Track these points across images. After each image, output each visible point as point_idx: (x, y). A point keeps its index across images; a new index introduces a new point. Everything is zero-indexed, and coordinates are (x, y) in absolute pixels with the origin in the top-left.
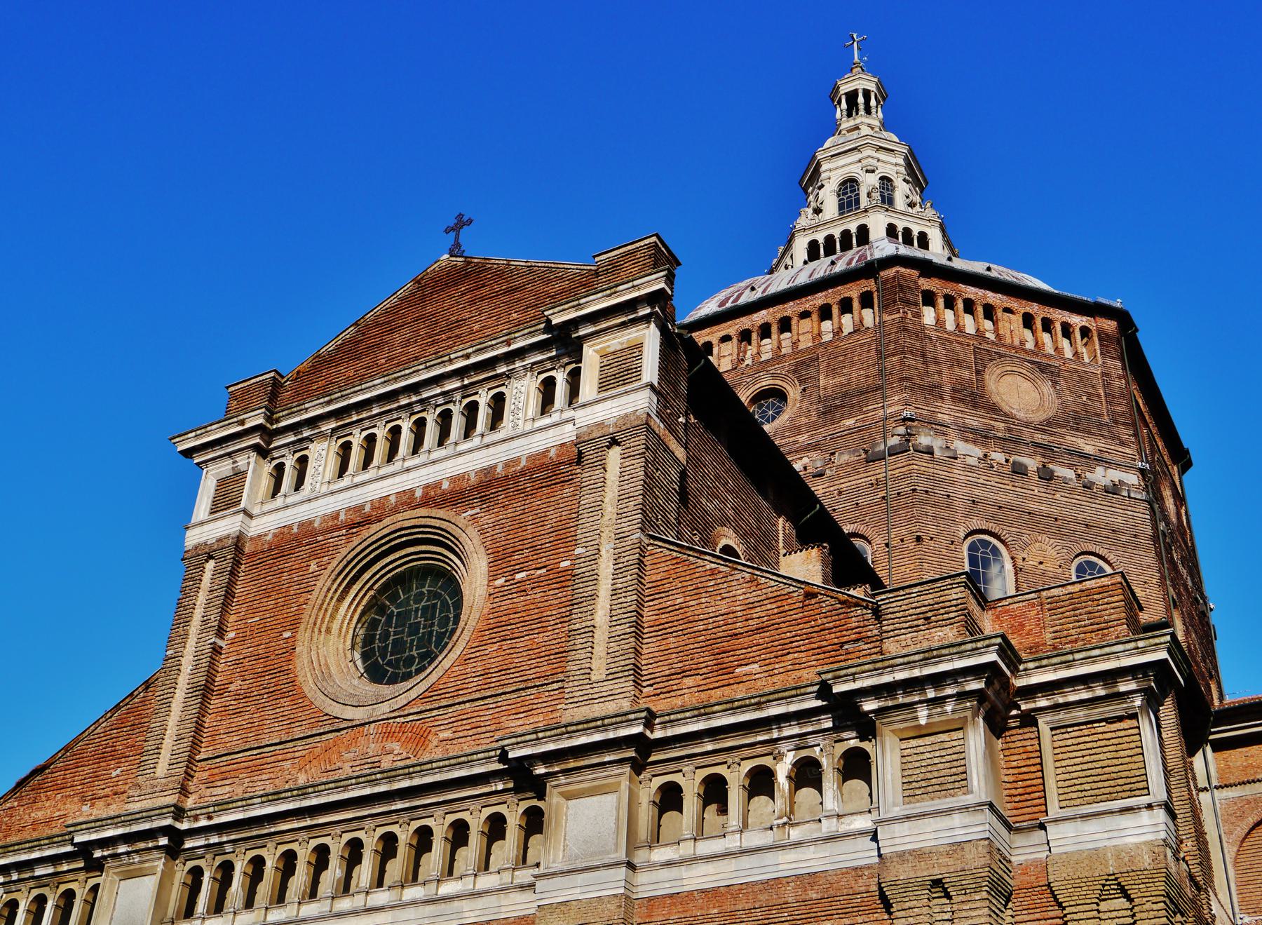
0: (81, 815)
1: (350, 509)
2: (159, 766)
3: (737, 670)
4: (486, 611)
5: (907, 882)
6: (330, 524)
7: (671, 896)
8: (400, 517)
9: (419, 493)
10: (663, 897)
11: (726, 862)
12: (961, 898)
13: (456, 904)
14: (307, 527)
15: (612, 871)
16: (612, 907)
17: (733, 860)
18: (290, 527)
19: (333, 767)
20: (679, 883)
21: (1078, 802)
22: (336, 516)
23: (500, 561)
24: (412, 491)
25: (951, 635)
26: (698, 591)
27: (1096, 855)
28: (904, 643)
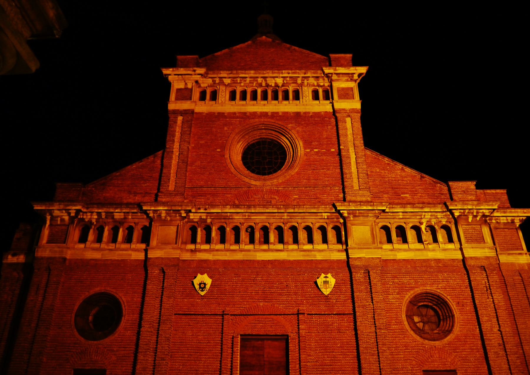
0: (130, 198)
1: (240, 113)
2: (170, 186)
3: (402, 195)
4: (304, 159)
5: (473, 266)
6: (232, 115)
7: (393, 260)
8: (262, 120)
9: (269, 114)
10: (390, 260)
11: (411, 252)
12: (489, 272)
13: (313, 253)
14: (221, 115)
15: (376, 250)
16: (378, 261)
17: (413, 252)
18: (214, 113)
19: (249, 200)
20: (395, 256)
21: (503, 249)
22: (235, 113)
23: (307, 144)
24: (266, 113)
25: (473, 198)
26: (384, 169)
27: (513, 264)
28: (459, 198)
